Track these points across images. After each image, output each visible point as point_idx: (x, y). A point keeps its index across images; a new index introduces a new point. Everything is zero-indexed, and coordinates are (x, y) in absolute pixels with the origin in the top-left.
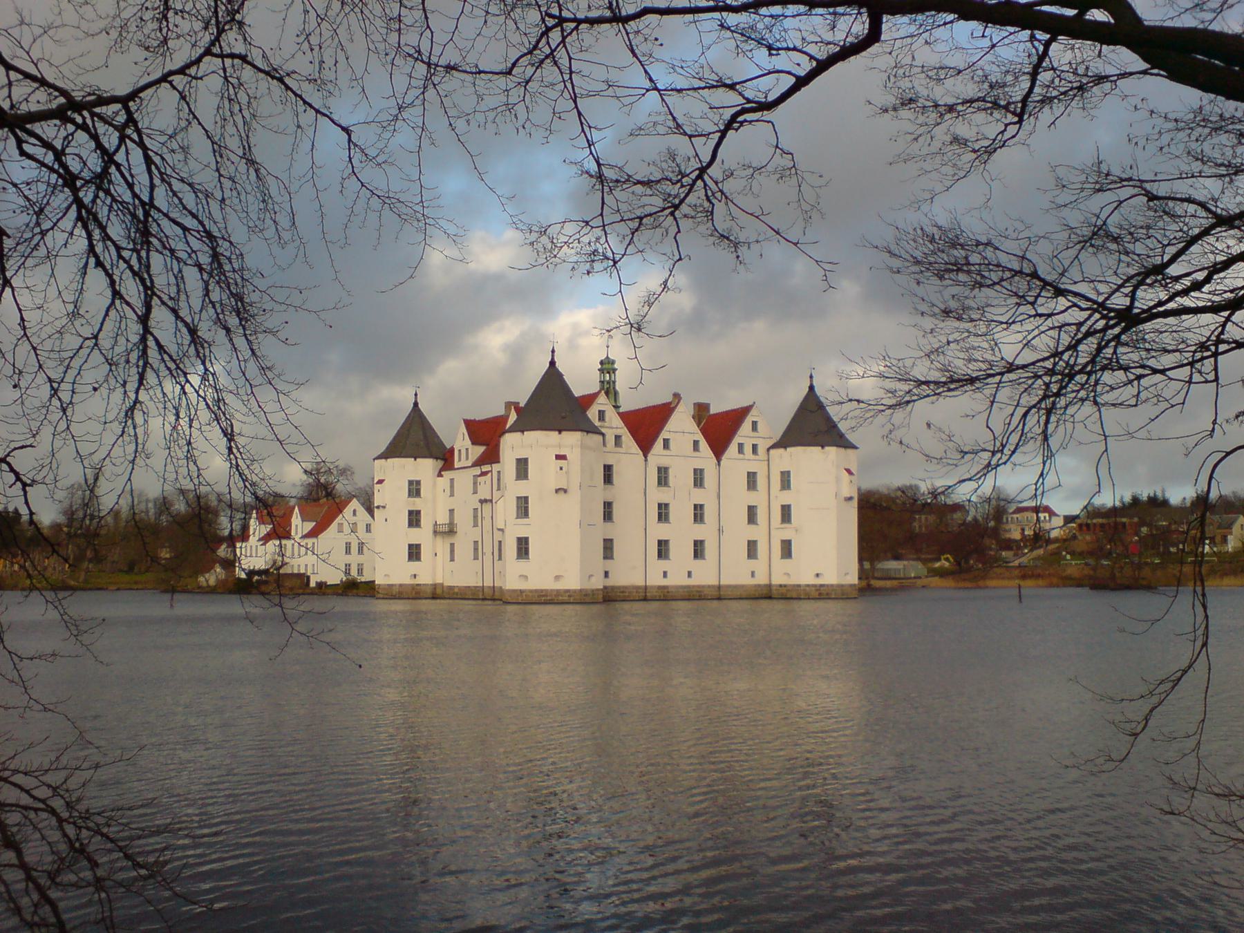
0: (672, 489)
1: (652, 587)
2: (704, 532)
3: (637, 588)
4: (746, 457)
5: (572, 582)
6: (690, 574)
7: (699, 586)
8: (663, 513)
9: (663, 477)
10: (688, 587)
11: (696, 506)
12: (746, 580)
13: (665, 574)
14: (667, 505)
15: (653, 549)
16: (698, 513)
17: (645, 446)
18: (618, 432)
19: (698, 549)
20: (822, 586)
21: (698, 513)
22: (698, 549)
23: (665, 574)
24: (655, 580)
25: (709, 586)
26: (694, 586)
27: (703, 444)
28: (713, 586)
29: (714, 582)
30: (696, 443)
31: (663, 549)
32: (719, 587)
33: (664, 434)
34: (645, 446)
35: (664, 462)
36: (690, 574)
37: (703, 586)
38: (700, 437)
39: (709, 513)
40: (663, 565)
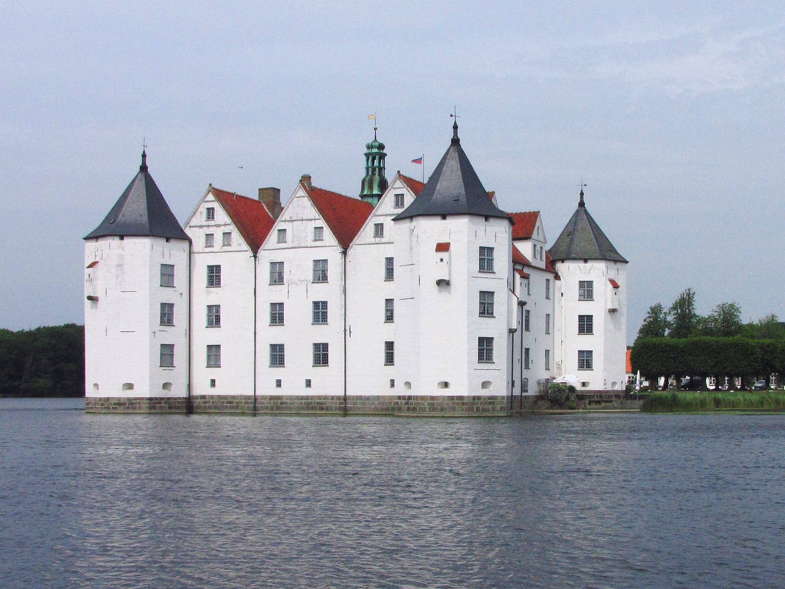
0: (286, 285)
1: (263, 397)
2: (329, 334)
3: (248, 397)
4: (383, 240)
5: (143, 390)
6: (308, 383)
7: (320, 397)
8: (277, 316)
9: (277, 276)
10: (307, 398)
11: (316, 304)
12: (385, 391)
13: (279, 383)
14: (281, 305)
15: (265, 355)
16: (277, 316)
17: (255, 243)
18: (227, 229)
19: (321, 355)
20: (410, 398)
21: (320, 312)
22: (321, 355)
23: (279, 383)
24: (266, 389)
25: (333, 398)
26: (313, 397)
27: (327, 233)
28: (339, 398)
29: (337, 391)
30: (319, 229)
31: (278, 355)
32: (345, 398)
33: (279, 225)
34: (255, 243)
35: (278, 257)
36: (308, 383)
37: (326, 397)
38: (322, 223)
39: (333, 312)
40: (278, 373)
